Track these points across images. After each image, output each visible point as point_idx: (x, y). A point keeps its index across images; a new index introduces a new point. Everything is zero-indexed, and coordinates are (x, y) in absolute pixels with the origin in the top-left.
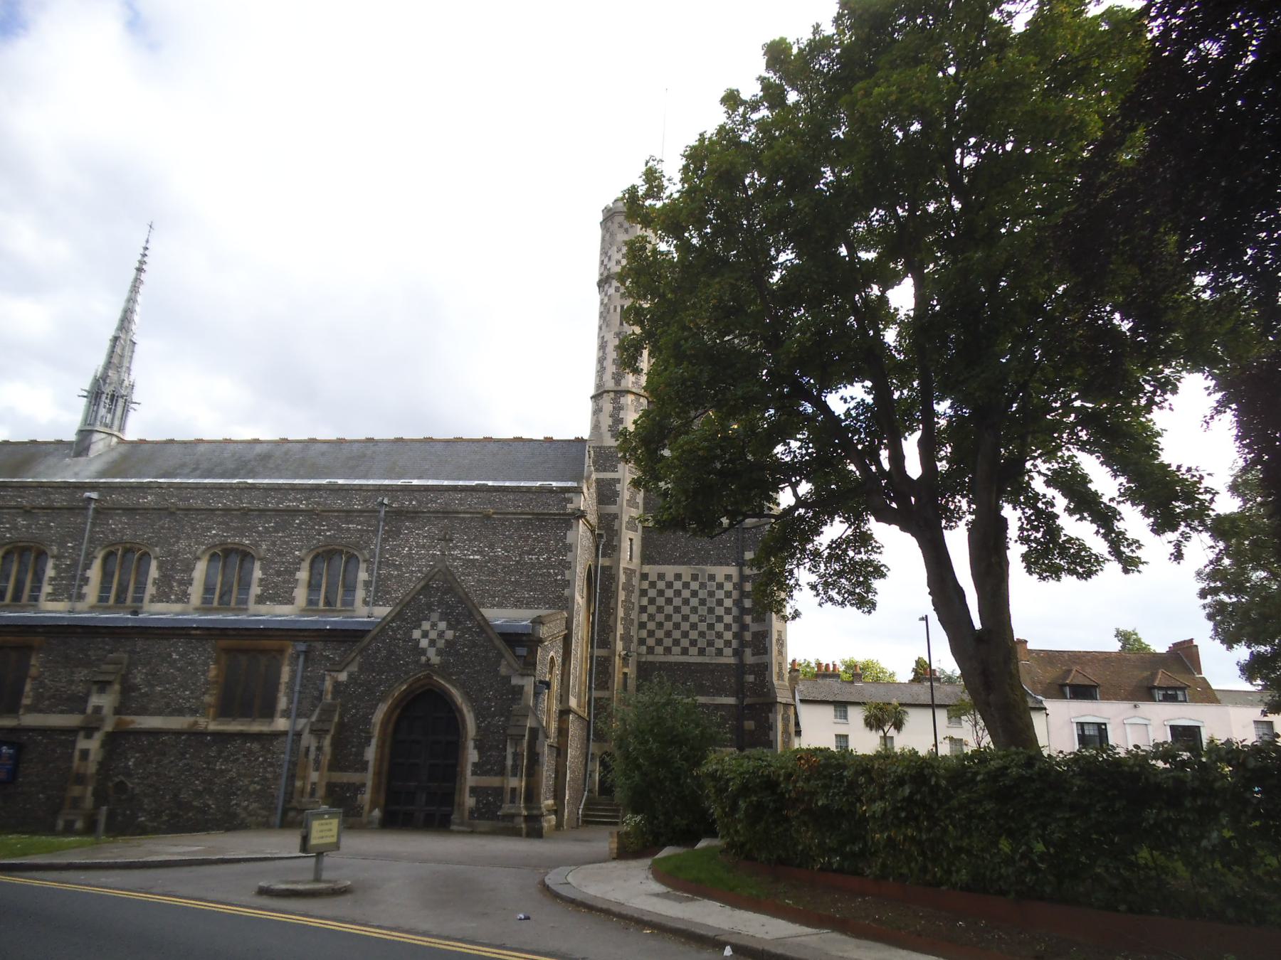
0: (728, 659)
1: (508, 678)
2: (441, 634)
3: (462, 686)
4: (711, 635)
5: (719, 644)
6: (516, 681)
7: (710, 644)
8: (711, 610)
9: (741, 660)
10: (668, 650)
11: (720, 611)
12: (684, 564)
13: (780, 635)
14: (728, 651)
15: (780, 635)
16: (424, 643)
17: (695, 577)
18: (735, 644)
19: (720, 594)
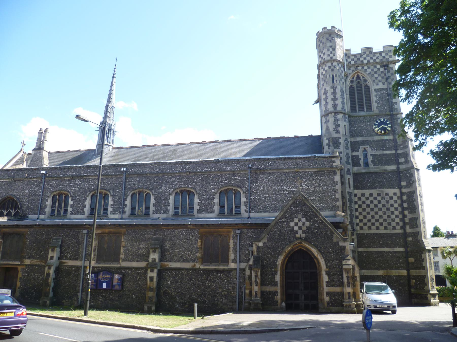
0: (398, 230)
1: (338, 243)
2: (304, 224)
3: (316, 247)
4: (389, 220)
5: (394, 224)
6: (341, 244)
7: (389, 224)
8: (388, 209)
9: (405, 230)
10: (370, 228)
11: (392, 209)
12: (373, 189)
13: (423, 219)
14: (398, 227)
15: (423, 219)
16: (296, 228)
17: (379, 195)
18: (401, 224)
19: (392, 202)
